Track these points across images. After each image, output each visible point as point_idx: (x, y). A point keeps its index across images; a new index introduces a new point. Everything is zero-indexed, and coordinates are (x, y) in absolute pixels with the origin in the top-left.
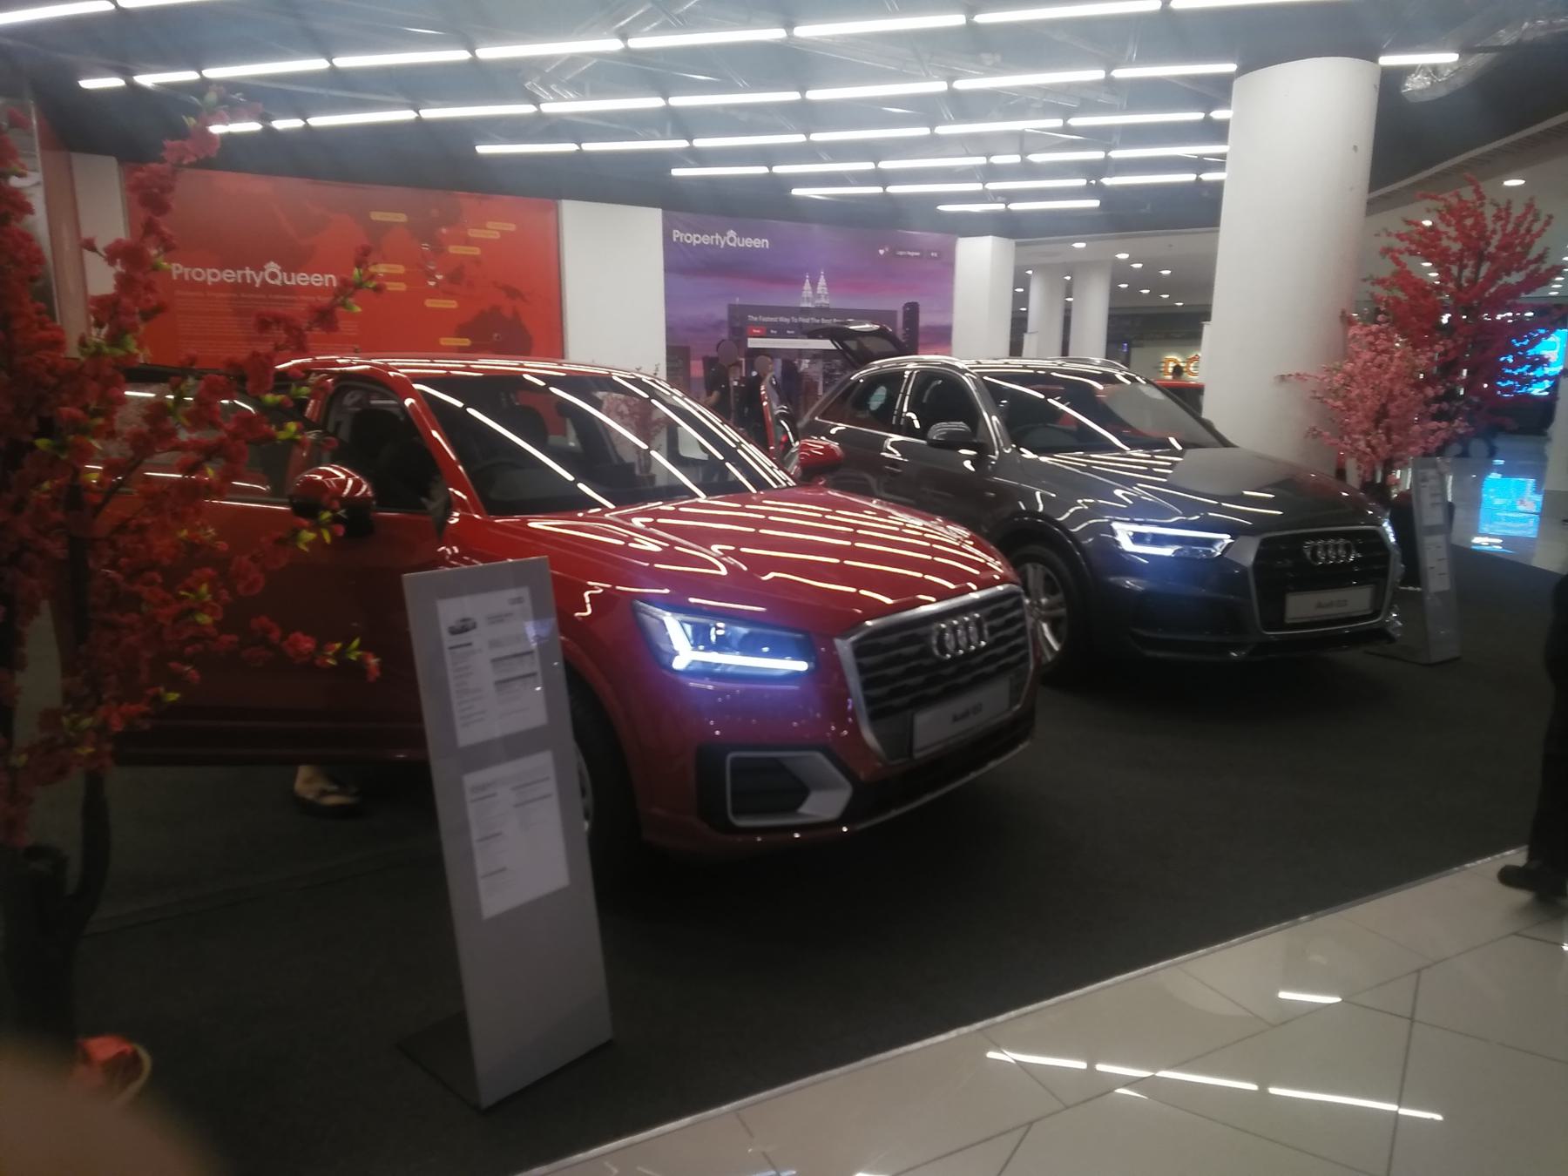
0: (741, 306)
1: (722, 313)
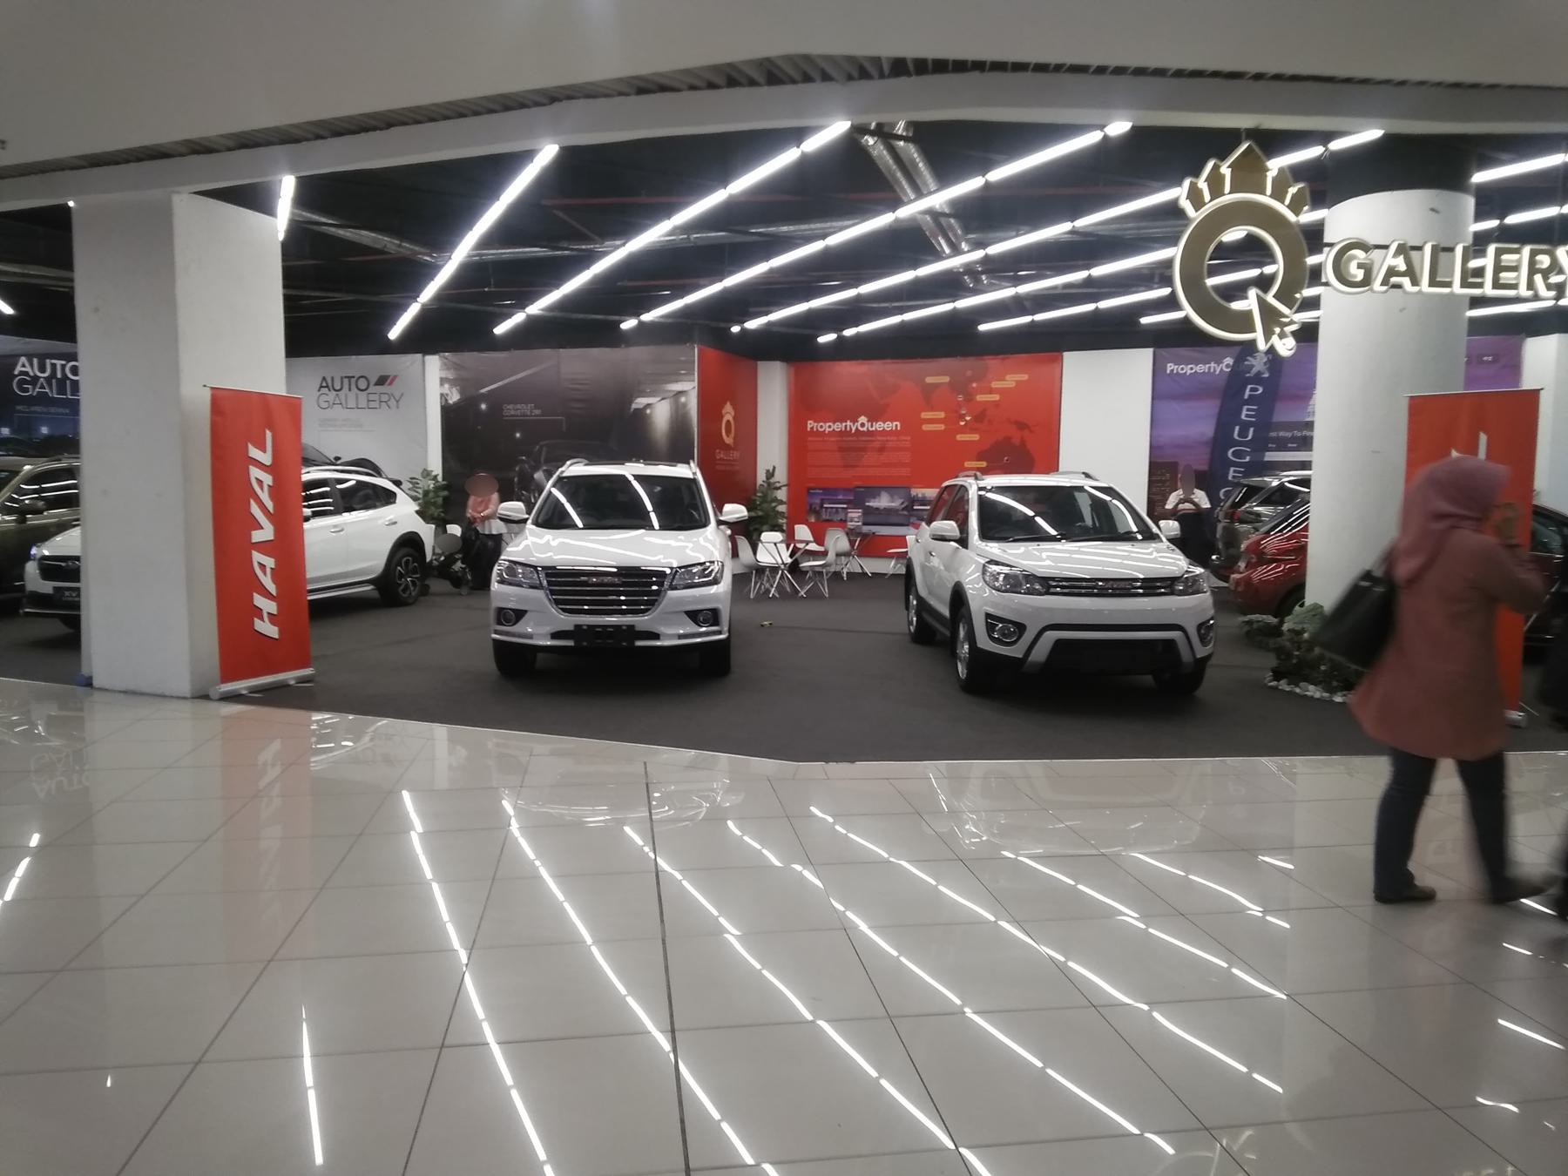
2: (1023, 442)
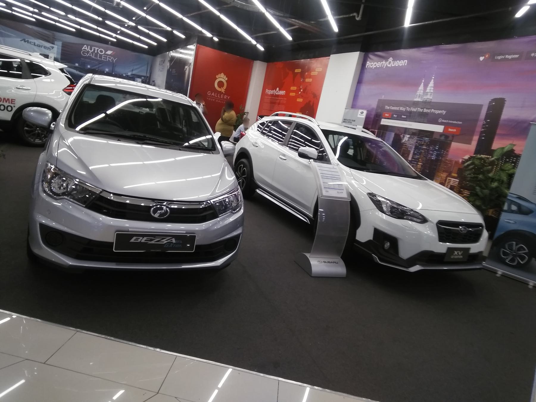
2: (313, 104)
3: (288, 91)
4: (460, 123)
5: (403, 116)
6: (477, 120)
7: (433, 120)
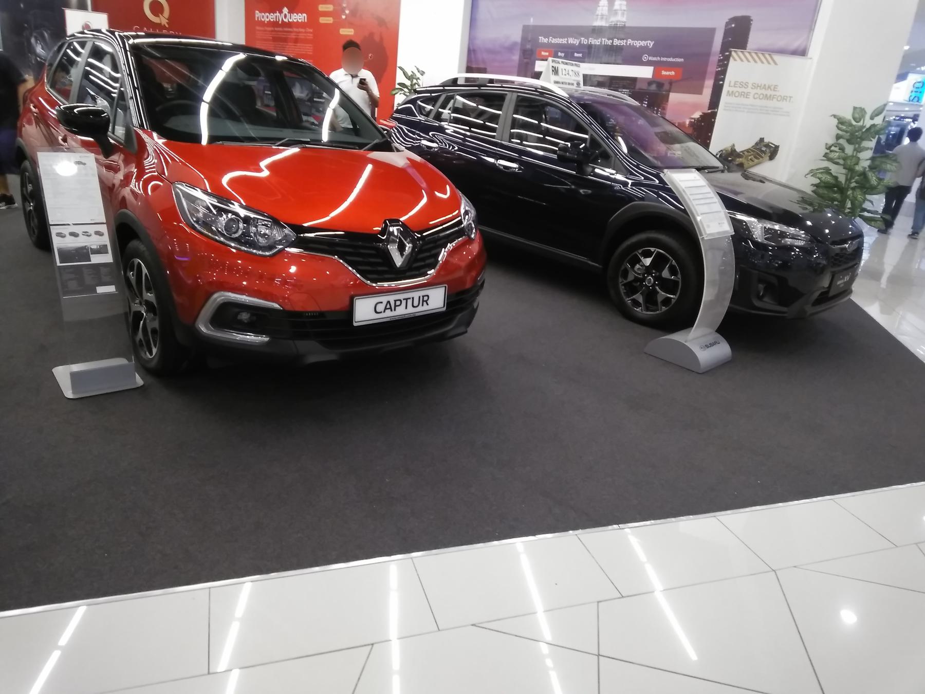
0: (535, 27)
1: (516, 35)
2: (381, 39)
3: (314, 16)
4: (682, 60)
5: (576, 55)
6: (708, 55)
7: (634, 58)
